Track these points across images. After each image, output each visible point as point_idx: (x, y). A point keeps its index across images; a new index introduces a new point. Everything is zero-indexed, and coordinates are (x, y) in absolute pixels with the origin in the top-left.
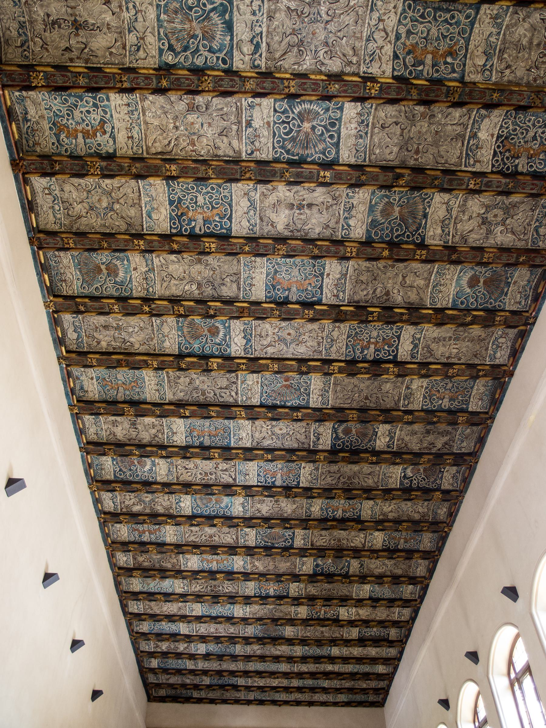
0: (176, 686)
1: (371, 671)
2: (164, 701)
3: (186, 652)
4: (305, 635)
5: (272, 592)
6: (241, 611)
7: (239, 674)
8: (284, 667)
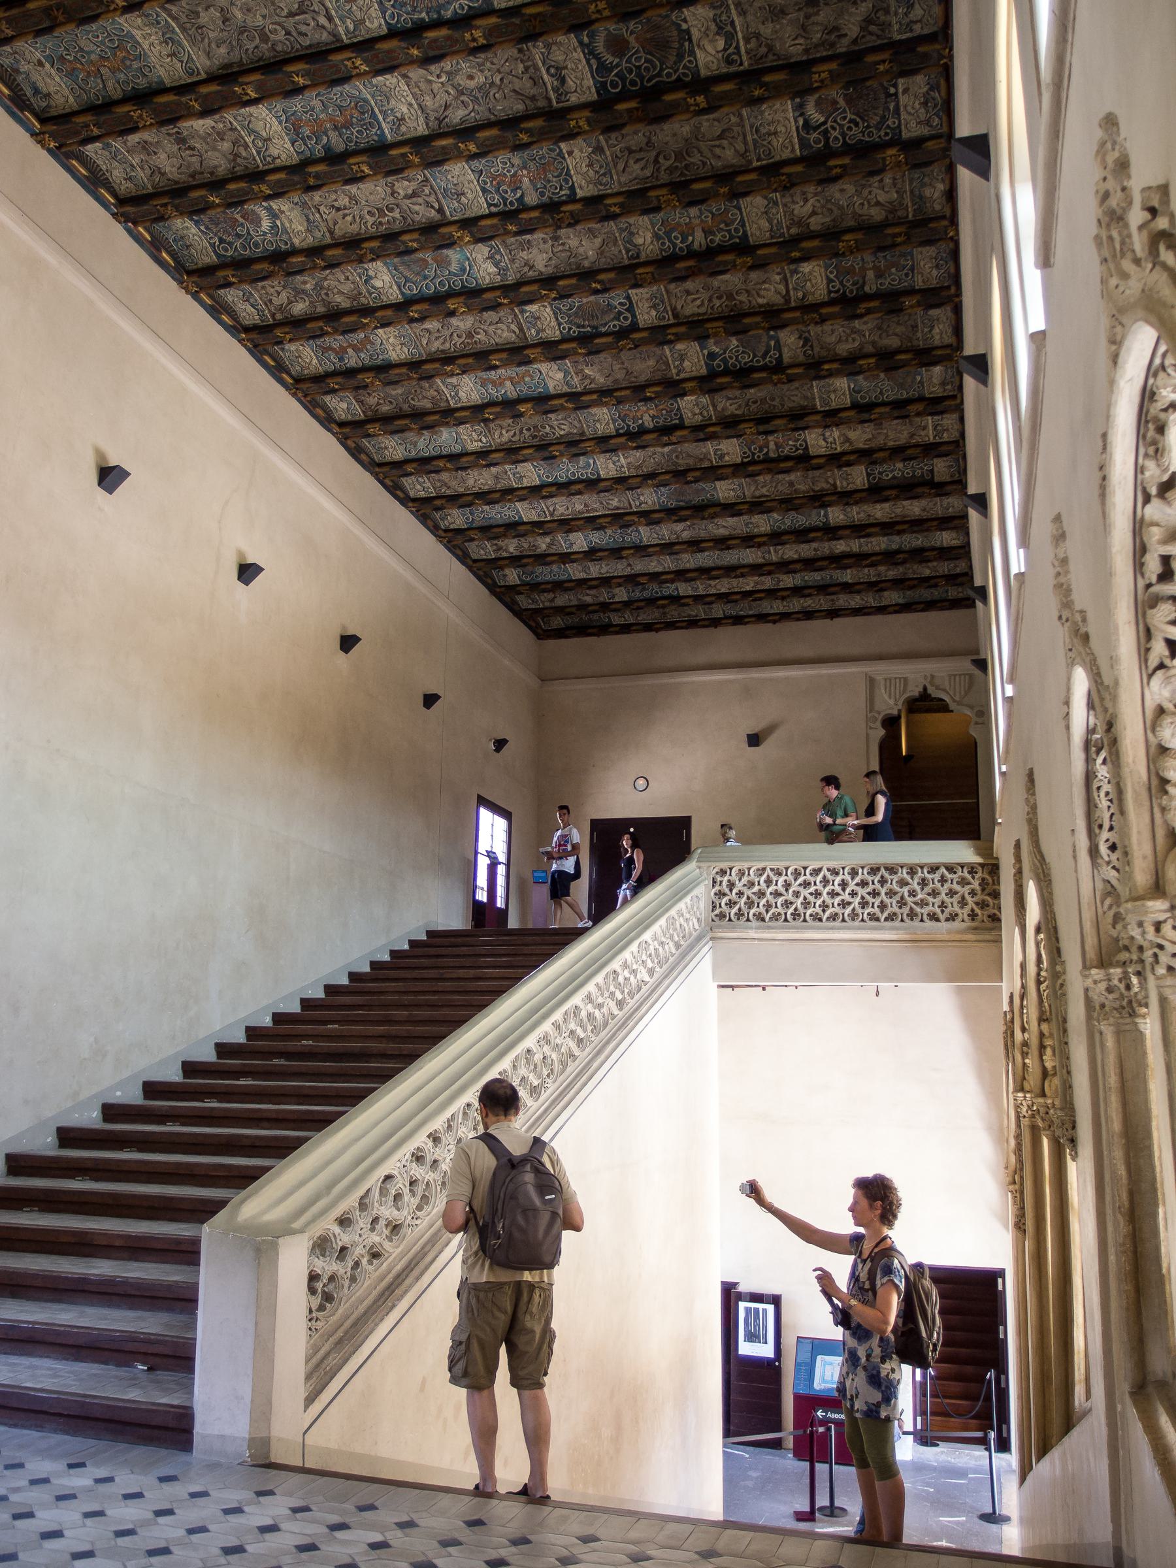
0: (568, 610)
1: (927, 544)
2: (566, 637)
3: (552, 551)
4: (757, 493)
5: (648, 422)
6: (611, 465)
7: (669, 577)
8: (750, 556)
